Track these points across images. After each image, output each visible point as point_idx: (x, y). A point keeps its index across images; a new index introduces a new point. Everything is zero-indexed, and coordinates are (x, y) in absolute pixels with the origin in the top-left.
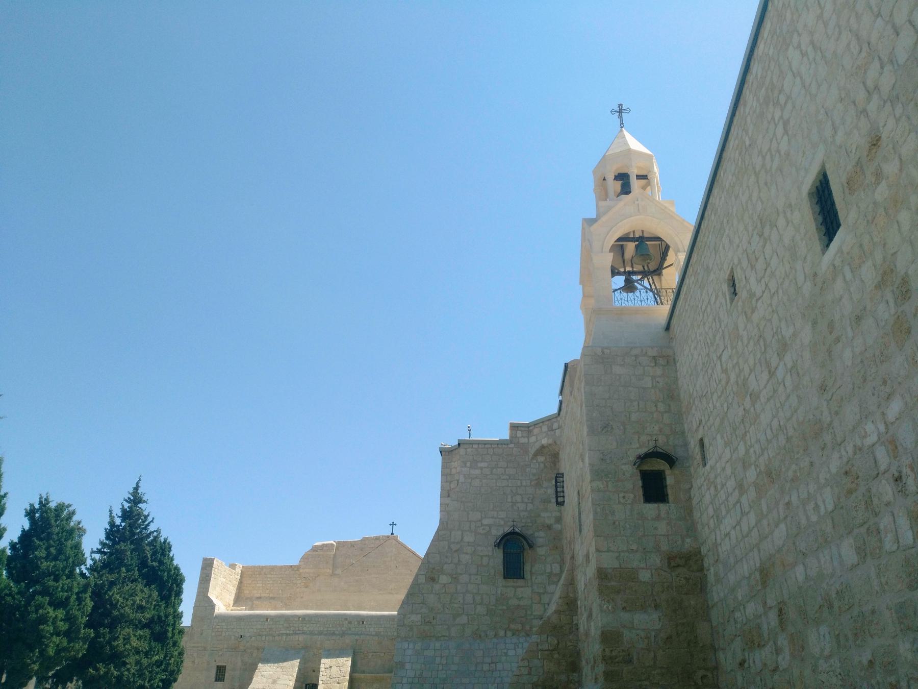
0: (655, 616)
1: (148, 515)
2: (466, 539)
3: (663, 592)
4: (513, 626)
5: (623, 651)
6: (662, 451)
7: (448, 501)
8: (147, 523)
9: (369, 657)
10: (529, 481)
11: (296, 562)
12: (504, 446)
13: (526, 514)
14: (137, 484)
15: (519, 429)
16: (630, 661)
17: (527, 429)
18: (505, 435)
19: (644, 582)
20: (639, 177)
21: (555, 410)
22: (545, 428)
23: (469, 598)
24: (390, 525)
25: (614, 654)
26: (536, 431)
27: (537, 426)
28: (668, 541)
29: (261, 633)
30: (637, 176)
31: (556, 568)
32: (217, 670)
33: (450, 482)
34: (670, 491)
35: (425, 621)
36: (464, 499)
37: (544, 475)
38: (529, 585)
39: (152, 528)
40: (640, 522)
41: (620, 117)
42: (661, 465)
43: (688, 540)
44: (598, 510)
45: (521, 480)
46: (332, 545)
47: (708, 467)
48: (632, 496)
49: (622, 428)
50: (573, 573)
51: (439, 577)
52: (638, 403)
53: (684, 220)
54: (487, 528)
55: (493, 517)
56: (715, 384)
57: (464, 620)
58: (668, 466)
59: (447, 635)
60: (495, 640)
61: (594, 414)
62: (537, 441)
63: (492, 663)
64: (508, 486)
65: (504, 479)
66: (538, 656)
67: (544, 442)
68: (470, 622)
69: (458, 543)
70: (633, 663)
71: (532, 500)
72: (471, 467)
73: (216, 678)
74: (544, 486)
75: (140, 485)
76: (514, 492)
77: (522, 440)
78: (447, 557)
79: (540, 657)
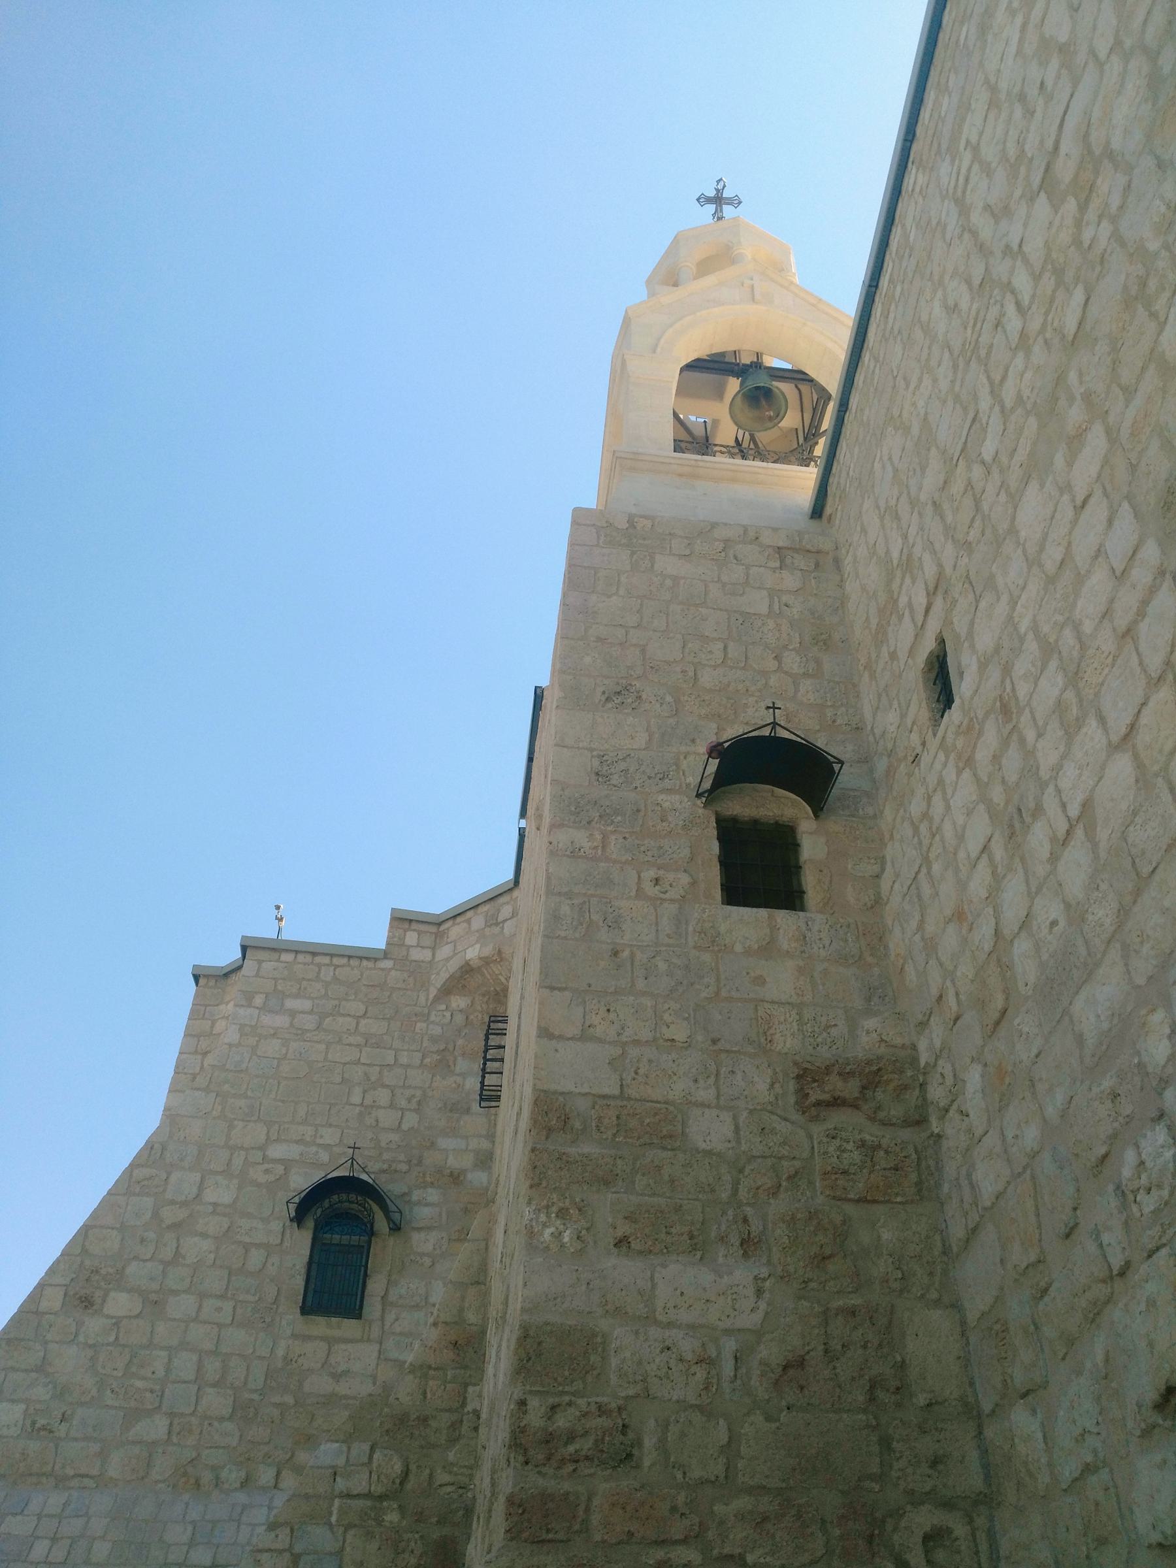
0: (742, 1275)
2: (210, 1196)
3: (775, 1192)
5: (602, 1410)
12: (365, 963)
13: (394, 1137)
15: (414, 926)
16: (626, 1458)
17: (433, 929)
19: (709, 1153)
21: (510, 875)
23: (185, 1364)
25: (562, 1422)
27: (459, 919)
28: (800, 1022)
33: (205, 1054)
35: (34, 1423)
36: (226, 1087)
37: (460, 1042)
38: (375, 1331)
40: (707, 957)
43: (871, 1023)
44: (565, 909)
45: (397, 1051)
48: (685, 879)
51: (106, 1295)
52: (725, 647)
60: (241, 1497)
61: (588, 660)
64: (358, 1062)
65: (350, 1045)
66: (331, 1514)
67: (472, 953)
68: (175, 1439)
69: (184, 1204)
70: (638, 1467)
71: (419, 1103)
72: (265, 1009)
74: (458, 1070)
76: (373, 1079)
77: (416, 955)
78: (142, 1240)
79: (334, 1519)
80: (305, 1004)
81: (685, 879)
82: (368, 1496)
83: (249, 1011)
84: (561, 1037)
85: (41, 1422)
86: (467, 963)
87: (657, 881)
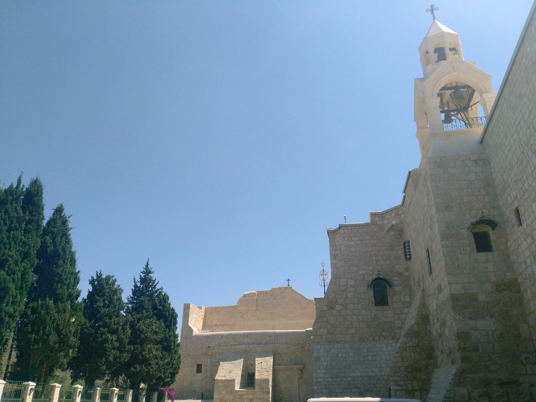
1: (155, 280)
2: (350, 283)
3: (494, 307)
4: (383, 334)
6: (488, 219)
7: (335, 261)
8: (155, 284)
9: (283, 356)
10: (386, 247)
11: (235, 304)
12: (368, 227)
14: (147, 263)
15: (377, 216)
16: (477, 350)
17: (381, 216)
18: (367, 219)
19: (482, 301)
20: (451, 49)
21: (399, 202)
22: (393, 214)
24: (287, 280)
25: (466, 346)
26: (387, 216)
27: (388, 213)
29: (220, 345)
30: (449, 49)
31: (408, 298)
32: (197, 366)
33: (336, 250)
34: (493, 244)
35: (329, 332)
36: (346, 260)
37: (394, 243)
39: (158, 287)
41: (432, 13)
42: (486, 228)
43: (508, 274)
46: (255, 293)
47: (524, 225)
48: (469, 248)
49: (458, 206)
50: (424, 300)
53: (484, 73)
54: (362, 276)
55: (365, 270)
56: (530, 170)
57: (353, 331)
58: (491, 228)
59: (344, 340)
62: (388, 223)
63: (374, 356)
64: (373, 250)
66: (407, 350)
67: (394, 222)
70: (479, 351)
73: (197, 371)
75: (149, 263)
78: (339, 294)
79: (408, 351)
80: (356, 239)
81: (469, 248)
82: (413, 346)
83: (345, 241)
84: (453, 284)
85: (331, 332)
86: (393, 225)
87: (464, 250)
